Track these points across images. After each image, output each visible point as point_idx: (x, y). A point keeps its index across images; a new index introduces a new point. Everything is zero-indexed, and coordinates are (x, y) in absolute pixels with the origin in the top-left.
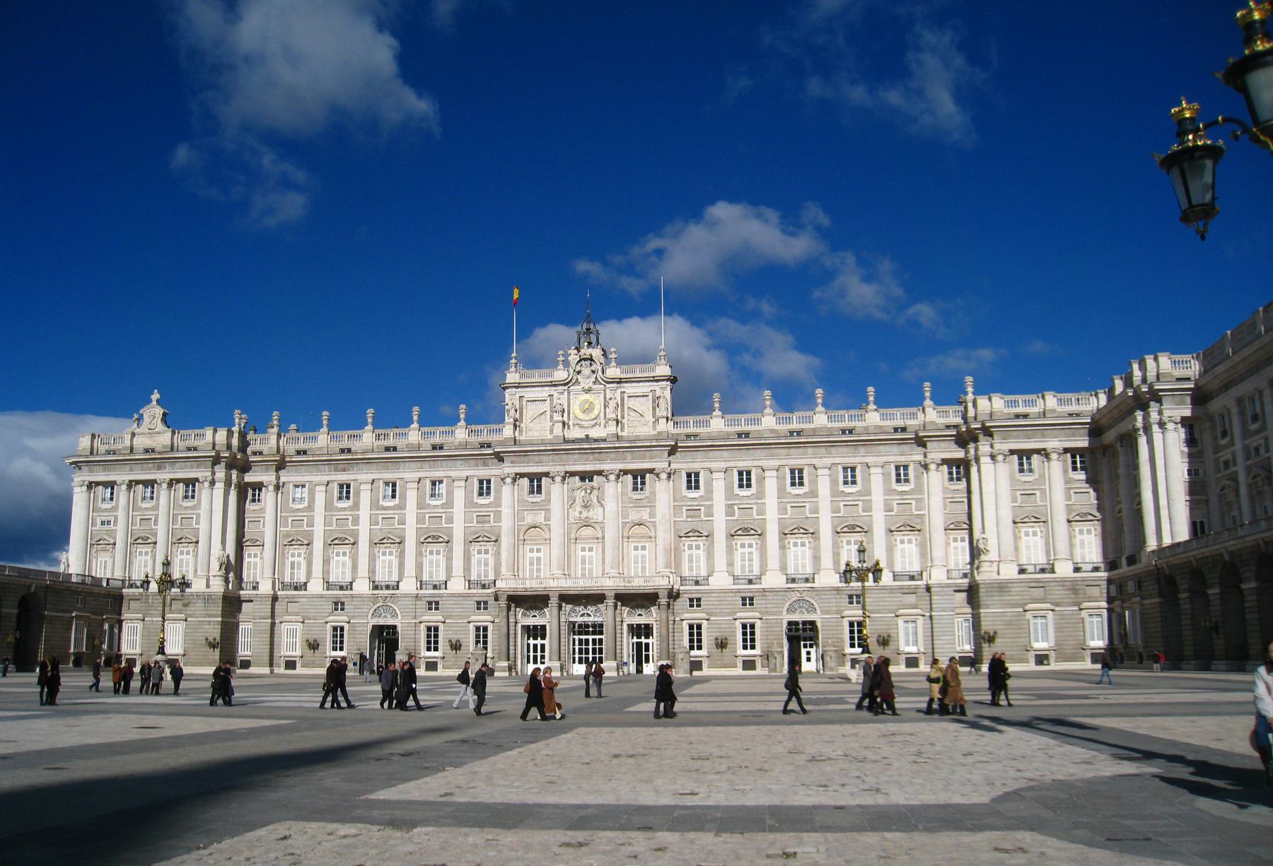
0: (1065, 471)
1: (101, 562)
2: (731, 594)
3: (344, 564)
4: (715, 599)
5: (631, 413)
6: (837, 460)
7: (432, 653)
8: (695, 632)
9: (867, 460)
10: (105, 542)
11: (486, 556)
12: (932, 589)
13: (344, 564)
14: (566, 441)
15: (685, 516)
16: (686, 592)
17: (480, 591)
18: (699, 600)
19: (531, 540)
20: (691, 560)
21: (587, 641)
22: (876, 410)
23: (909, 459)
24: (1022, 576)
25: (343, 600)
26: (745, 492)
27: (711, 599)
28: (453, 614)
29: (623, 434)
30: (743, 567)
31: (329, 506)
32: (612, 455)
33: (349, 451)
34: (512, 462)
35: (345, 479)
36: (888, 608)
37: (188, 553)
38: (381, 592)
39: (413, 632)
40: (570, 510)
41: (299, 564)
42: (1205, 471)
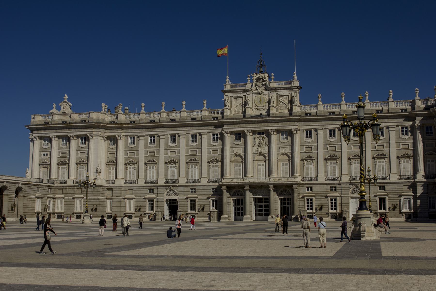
1: (44, 172)
2: (326, 185)
3: (153, 172)
4: (318, 187)
5: (280, 103)
7: (193, 212)
9: (388, 124)
10: (45, 163)
11: (216, 168)
12: (417, 184)
14: (252, 117)
15: (305, 150)
16: (305, 184)
17: (214, 184)
18: (311, 188)
19: (236, 161)
20: (308, 170)
21: (261, 206)
22: (393, 101)
23: (408, 124)
25: (153, 188)
26: (333, 139)
27: (317, 187)
28: (202, 194)
29: (277, 113)
30: (331, 173)
33: (154, 121)
34: (227, 126)
35: (152, 134)
36: (396, 192)
37: (83, 168)
38: (170, 184)
39: (184, 202)
40: (254, 147)
41: (133, 172)
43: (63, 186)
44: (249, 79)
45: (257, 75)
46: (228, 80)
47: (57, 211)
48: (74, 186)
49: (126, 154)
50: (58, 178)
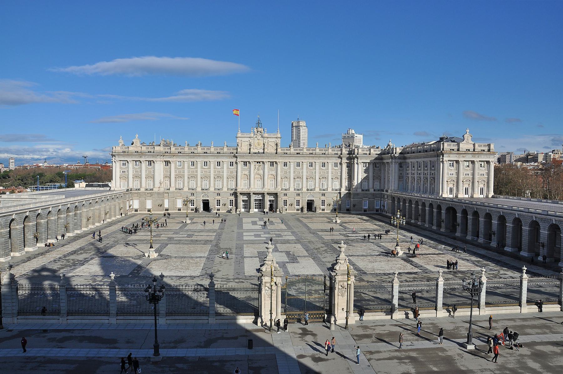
0: (374, 167)
3: (193, 183)
6: (321, 161)
7: (218, 207)
8: (285, 202)
13: (193, 183)
17: (231, 191)
20: (284, 184)
21: (257, 203)
24: (362, 192)
31: (189, 168)
32: (266, 157)
34: (240, 158)
37: (150, 181)
41: (180, 183)
42: (403, 174)
43: (138, 192)
44: (252, 131)
45: (257, 129)
46: (239, 130)
47: (134, 207)
48: (145, 192)
49: (176, 172)
50: (133, 187)
